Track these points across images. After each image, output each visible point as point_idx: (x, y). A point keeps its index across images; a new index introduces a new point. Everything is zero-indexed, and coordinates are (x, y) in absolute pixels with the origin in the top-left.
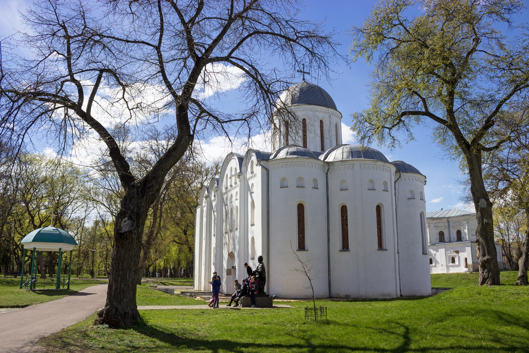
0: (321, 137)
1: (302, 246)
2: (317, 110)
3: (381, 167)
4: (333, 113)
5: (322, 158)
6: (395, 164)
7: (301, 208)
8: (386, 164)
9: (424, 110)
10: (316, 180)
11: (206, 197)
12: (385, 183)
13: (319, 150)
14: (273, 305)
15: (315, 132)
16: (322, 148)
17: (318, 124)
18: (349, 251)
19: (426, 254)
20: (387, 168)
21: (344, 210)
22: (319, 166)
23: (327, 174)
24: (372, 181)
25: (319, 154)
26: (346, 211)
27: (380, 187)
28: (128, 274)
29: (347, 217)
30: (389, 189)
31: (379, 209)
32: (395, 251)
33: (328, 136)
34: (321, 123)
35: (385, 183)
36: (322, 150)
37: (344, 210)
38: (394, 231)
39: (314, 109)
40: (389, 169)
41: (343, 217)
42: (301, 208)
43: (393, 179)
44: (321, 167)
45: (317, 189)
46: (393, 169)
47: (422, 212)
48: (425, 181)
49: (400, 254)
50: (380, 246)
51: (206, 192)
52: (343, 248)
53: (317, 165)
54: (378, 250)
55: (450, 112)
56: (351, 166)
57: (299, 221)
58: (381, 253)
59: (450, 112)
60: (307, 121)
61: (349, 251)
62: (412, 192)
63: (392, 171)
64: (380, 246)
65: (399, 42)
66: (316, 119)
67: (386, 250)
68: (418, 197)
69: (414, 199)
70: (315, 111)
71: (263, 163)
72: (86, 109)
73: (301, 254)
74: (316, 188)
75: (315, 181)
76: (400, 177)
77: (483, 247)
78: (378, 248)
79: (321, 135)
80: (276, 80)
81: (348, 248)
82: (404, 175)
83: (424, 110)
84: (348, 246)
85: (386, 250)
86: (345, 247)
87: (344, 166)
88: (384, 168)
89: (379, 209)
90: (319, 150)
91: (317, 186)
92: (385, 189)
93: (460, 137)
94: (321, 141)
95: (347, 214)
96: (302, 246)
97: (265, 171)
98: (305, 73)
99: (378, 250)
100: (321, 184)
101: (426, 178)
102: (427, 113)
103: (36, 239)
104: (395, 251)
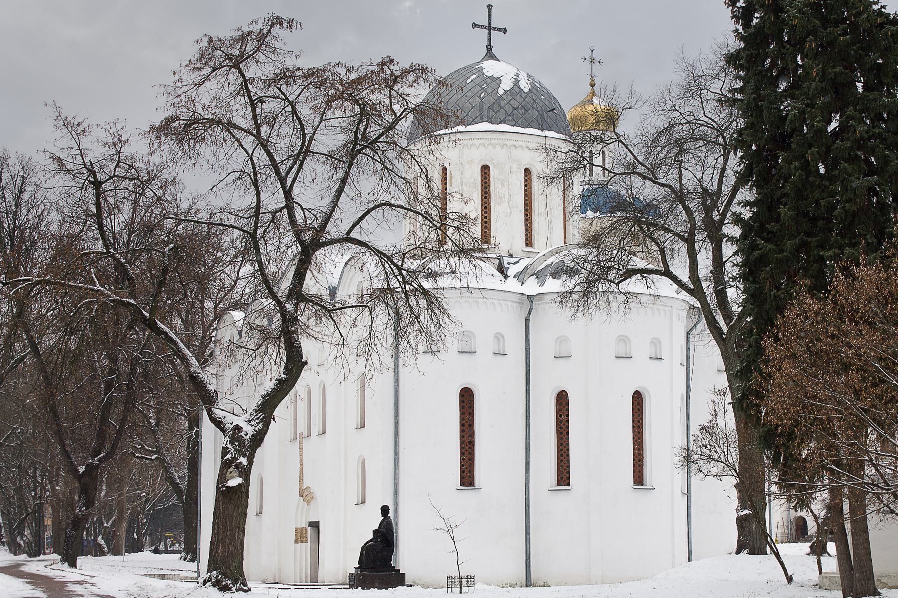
0: (526, 210)
1: (468, 478)
2: (517, 143)
7: (467, 397)
10: (503, 337)
15: (510, 201)
16: (526, 239)
17: (521, 176)
21: (562, 400)
22: (510, 304)
26: (567, 404)
27: (641, 350)
28: (237, 534)
29: (568, 415)
31: (638, 399)
33: (542, 209)
34: (525, 176)
36: (527, 245)
37: (562, 400)
39: (509, 143)
41: (561, 416)
42: (467, 397)
44: (515, 305)
50: (639, 478)
53: (503, 303)
57: (462, 425)
60: (493, 173)
66: (515, 167)
70: (513, 148)
73: (468, 494)
75: (499, 337)
79: (526, 205)
80: (414, 246)
81: (568, 484)
84: (569, 478)
89: (638, 399)
94: (526, 220)
95: (568, 410)
96: (468, 478)
102: (667, 273)
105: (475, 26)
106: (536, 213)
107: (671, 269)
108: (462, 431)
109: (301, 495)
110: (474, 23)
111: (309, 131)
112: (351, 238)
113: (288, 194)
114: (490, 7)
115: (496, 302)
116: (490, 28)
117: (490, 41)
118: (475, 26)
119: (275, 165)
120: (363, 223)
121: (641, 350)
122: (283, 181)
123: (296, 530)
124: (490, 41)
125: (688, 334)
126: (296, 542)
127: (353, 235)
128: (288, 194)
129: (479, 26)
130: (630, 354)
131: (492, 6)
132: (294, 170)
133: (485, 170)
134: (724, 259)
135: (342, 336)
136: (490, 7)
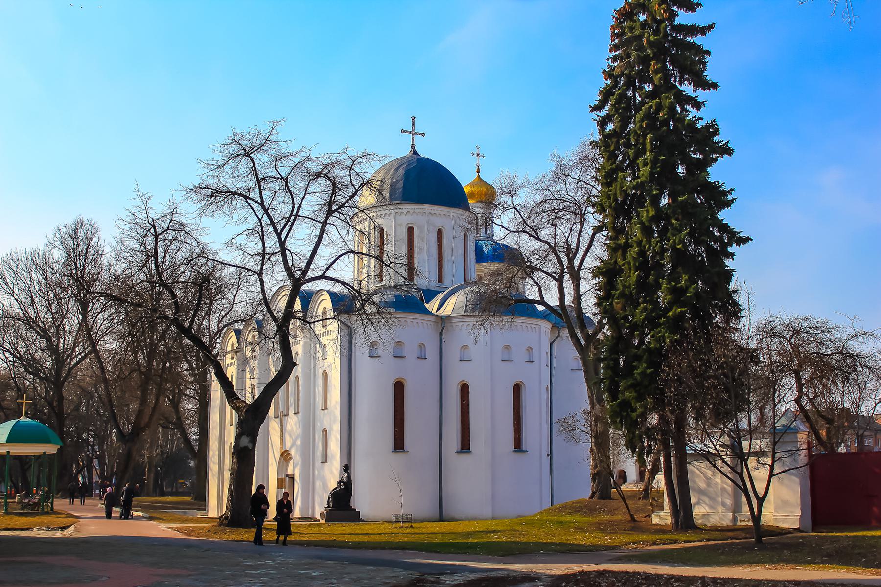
1: (399, 445)
2: (432, 212)
9: (538, 299)
13: (433, 285)
17: (435, 235)
18: (470, 452)
20: (533, 326)
22: (429, 323)
23: (441, 334)
27: (519, 355)
31: (517, 389)
36: (439, 282)
37: (465, 389)
50: (518, 446)
51: (234, 339)
52: (462, 448)
54: (515, 451)
60: (416, 232)
61: (470, 452)
65: (508, 232)
66: (431, 228)
71: (344, 317)
73: (400, 456)
74: (423, 357)
75: (422, 346)
86: (465, 446)
88: (529, 326)
89: (517, 389)
97: (346, 331)
98: (416, 133)
99: (515, 451)
100: (432, 353)
105: (403, 131)
106: (446, 260)
107: (545, 300)
108: (396, 411)
109: (282, 455)
110: (402, 129)
111: (297, 201)
112: (326, 276)
113: (282, 243)
114: (413, 118)
116: (413, 133)
117: (413, 141)
118: (403, 131)
119: (272, 223)
120: (335, 265)
121: (519, 355)
122: (279, 235)
123: (278, 479)
124: (413, 141)
125: (551, 344)
126: (278, 488)
127: (328, 274)
128: (282, 243)
129: (405, 131)
130: (533, 359)
131: (415, 118)
132: (288, 227)
133: (410, 230)
134: (581, 294)
136: (413, 118)
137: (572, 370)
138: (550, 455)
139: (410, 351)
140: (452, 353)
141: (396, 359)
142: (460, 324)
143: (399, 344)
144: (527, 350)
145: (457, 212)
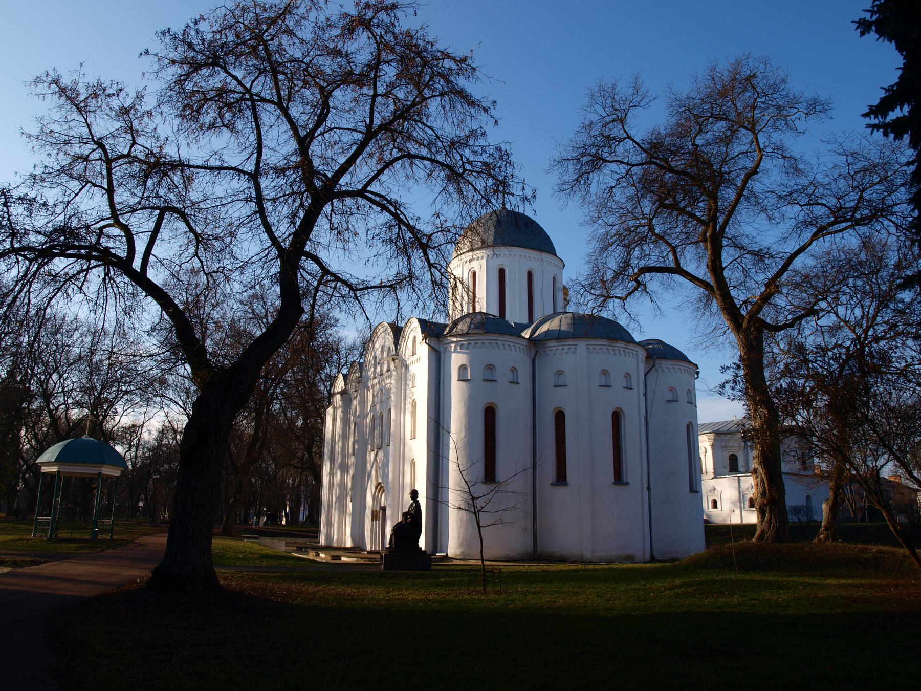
3: (622, 350)
4: (549, 261)
5: (526, 334)
6: (644, 344)
8: (631, 346)
9: (673, 265)
10: (515, 369)
11: (343, 393)
12: (628, 376)
13: (525, 321)
14: (433, 567)
19: (697, 492)
20: (631, 351)
22: (521, 347)
23: (534, 360)
24: (605, 373)
25: (524, 327)
27: (618, 381)
30: (634, 386)
31: (617, 417)
32: (642, 486)
35: (628, 376)
37: (560, 417)
38: (641, 454)
40: (634, 352)
43: (642, 368)
45: (517, 383)
46: (642, 354)
47: (690, 422)
48: (698, 373)
49: (652, 492)
50: (619, 478)
53: (517, 346)
54: (615, 483)
55: (716, 267)
56: (573, 347)
58: (617, 488)
59: (716, 267)
62: (672, 389)
63: (640, 356)
64: (619, 478)
67: (627, 484)
68: (683, 398)
69: (677, 401)
72: (139, 266)
75: (514, 370)
76: (654, 366)
77: (763, 482)
78: (613, 480)
82: (658, 362)
83: (673, 265)
84: (565, 476)
85: (627, 484)
86: (561, 478)
87: (561, 347)
88: (627, 350)
89: (617, 417)
90: (525, 321)
91: (517, 380)
92: (628, 385)
93: (730, 309)
99: (615, 483)
101: (698, 368)
102: (678, 270)
103: (60, 460)
104: (642, 486)
115: (511, 344)
121: (618, 381)
126: (372, 520)
134: (724, 266)
135: (368, 319)
137: (668, 401)
138: (649, 489)
139: (504, 375)
140: (547, 376)
141: (486, 382)
142: (554, 349)
143: (490, 367)
144: (625, 376)
145: (546, 257)
